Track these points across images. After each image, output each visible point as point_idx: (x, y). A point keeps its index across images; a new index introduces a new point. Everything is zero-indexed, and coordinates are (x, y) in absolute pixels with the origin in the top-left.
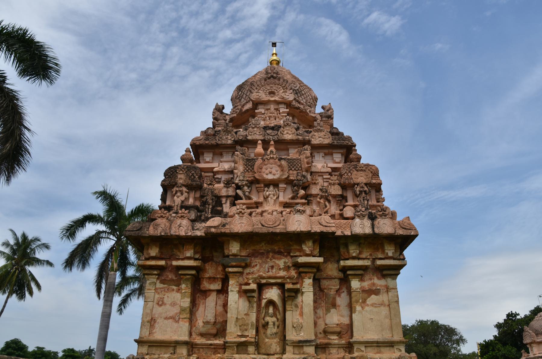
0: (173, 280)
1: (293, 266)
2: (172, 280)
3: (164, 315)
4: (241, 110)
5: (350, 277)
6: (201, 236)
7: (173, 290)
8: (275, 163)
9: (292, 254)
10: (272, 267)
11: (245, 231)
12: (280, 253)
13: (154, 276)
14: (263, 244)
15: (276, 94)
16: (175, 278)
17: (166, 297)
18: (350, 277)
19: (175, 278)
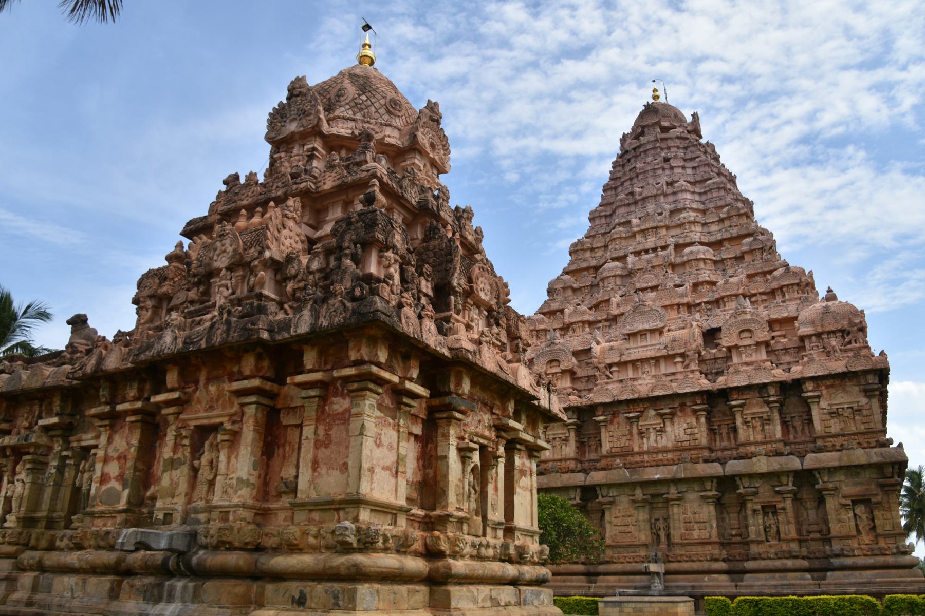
0: (389, 408)
1: (494, 426)
2: (387, 408)
3: (381, 463)
4: (383, 138)
5: (516, 451)
6: (446, 357)
7: (390, 424)
8: (489, 280)
9: (494, 411)
10: (480, 421)
11: (492, 370)
12: (485, 404)
13: (376, 396)
14: (478, 388)
15: (437, 151)
16: (391, 406)
17: (383, 432)
18: (516, 451)
19: (391, 406)
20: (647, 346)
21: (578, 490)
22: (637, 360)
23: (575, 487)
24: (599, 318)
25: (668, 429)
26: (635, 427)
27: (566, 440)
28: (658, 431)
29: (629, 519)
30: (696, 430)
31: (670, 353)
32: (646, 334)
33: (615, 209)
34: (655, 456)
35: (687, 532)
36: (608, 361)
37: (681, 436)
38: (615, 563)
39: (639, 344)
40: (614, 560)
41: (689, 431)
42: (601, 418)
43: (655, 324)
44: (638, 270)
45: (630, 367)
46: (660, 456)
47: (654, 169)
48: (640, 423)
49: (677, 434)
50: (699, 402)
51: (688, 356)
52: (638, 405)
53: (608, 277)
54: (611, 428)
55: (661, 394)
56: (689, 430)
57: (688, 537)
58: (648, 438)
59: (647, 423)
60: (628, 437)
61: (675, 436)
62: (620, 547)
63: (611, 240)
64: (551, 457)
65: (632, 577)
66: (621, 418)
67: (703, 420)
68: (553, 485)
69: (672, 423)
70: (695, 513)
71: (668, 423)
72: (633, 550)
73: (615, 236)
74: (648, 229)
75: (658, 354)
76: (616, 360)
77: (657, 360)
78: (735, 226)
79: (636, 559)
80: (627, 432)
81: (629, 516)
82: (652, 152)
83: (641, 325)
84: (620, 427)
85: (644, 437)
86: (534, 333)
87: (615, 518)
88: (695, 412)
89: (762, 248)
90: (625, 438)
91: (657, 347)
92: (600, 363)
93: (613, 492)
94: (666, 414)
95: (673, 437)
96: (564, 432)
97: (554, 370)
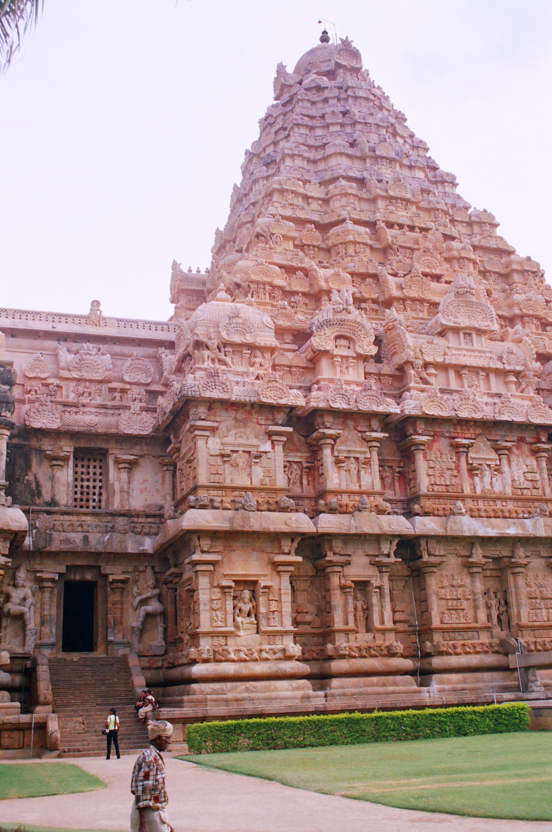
20: (473, 351)
21: (395, 543)
22: (465, 367)
23: (390, 537)
24: (367, 296)
25: (505, 468)
26: (463, 459)
27: (368, 463)
28: (495, 471)
29: (460, 590)
30: (537, 477)
31: (507, 367)
32: (470, 334)
33: (330, 156)
34: (491, 503)
35: (533, 611)
36: (429, 359)
37: (522, 482)
38: (450, 654)
39: (463, 346)
40: (450, 651)
41: (529, 476)
42: (425, 438)
43: (486, 324)
44: (401, 247)
45: (452, 374)
46: (499, 505)
47: (378, 126)
48: (470, 455)
49: (516, 478)
50: (543, 440)
51: (524, 376)
52: (468, 430)
53: (355, 243)
54: (431, 455)
55: (510, 419)
56: (529, 475)
57: (535, 619)
58: (482, 478)
59: (478, 456)
60: (455, 472)
61: (513, 481)
62: (454, 630)
63: (341, 195)
64: (344, 487)
65: (479, 675)
66: (443, 444)
67: (544, 464)
68: (367, 530)
69: (509, 461)
70: (541, 587)
71: (504, 462)
72: (470, 634)
73: (350, 191)
74: (396, 198)
75: (493, 365)
76: (440, 359)
77: (487, 371)
78: (489, 236)
79: (478, 649)
80: (453, 466)
81: (461, 586)
82: (364, 103)
83: (463, 321)
84: (444, 457)
85: (477, 475)
86: (268, 288)
87: (442, 588)
88: (535, 452)
89: (534, 273)
90: (449, 473)
91: (488, 355)
92: (416, 358)
93: (439, 550)
94: (505, 448)
95: (510, 482)
96: (363, 449)
97: (345, 352)
